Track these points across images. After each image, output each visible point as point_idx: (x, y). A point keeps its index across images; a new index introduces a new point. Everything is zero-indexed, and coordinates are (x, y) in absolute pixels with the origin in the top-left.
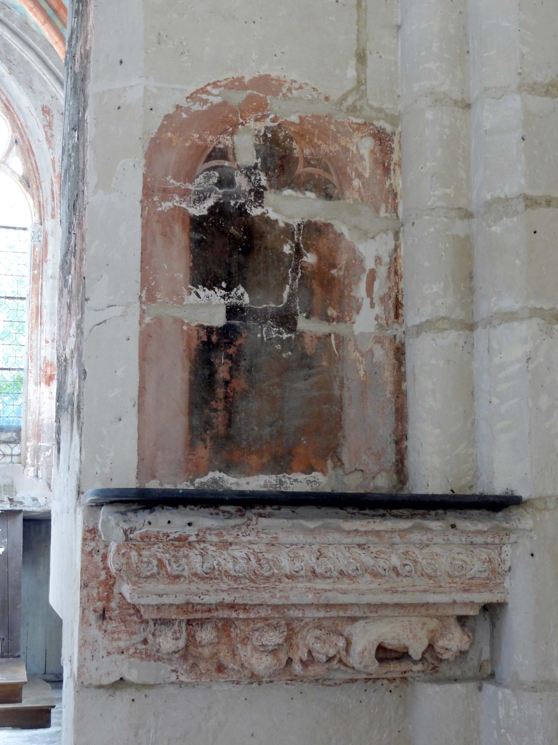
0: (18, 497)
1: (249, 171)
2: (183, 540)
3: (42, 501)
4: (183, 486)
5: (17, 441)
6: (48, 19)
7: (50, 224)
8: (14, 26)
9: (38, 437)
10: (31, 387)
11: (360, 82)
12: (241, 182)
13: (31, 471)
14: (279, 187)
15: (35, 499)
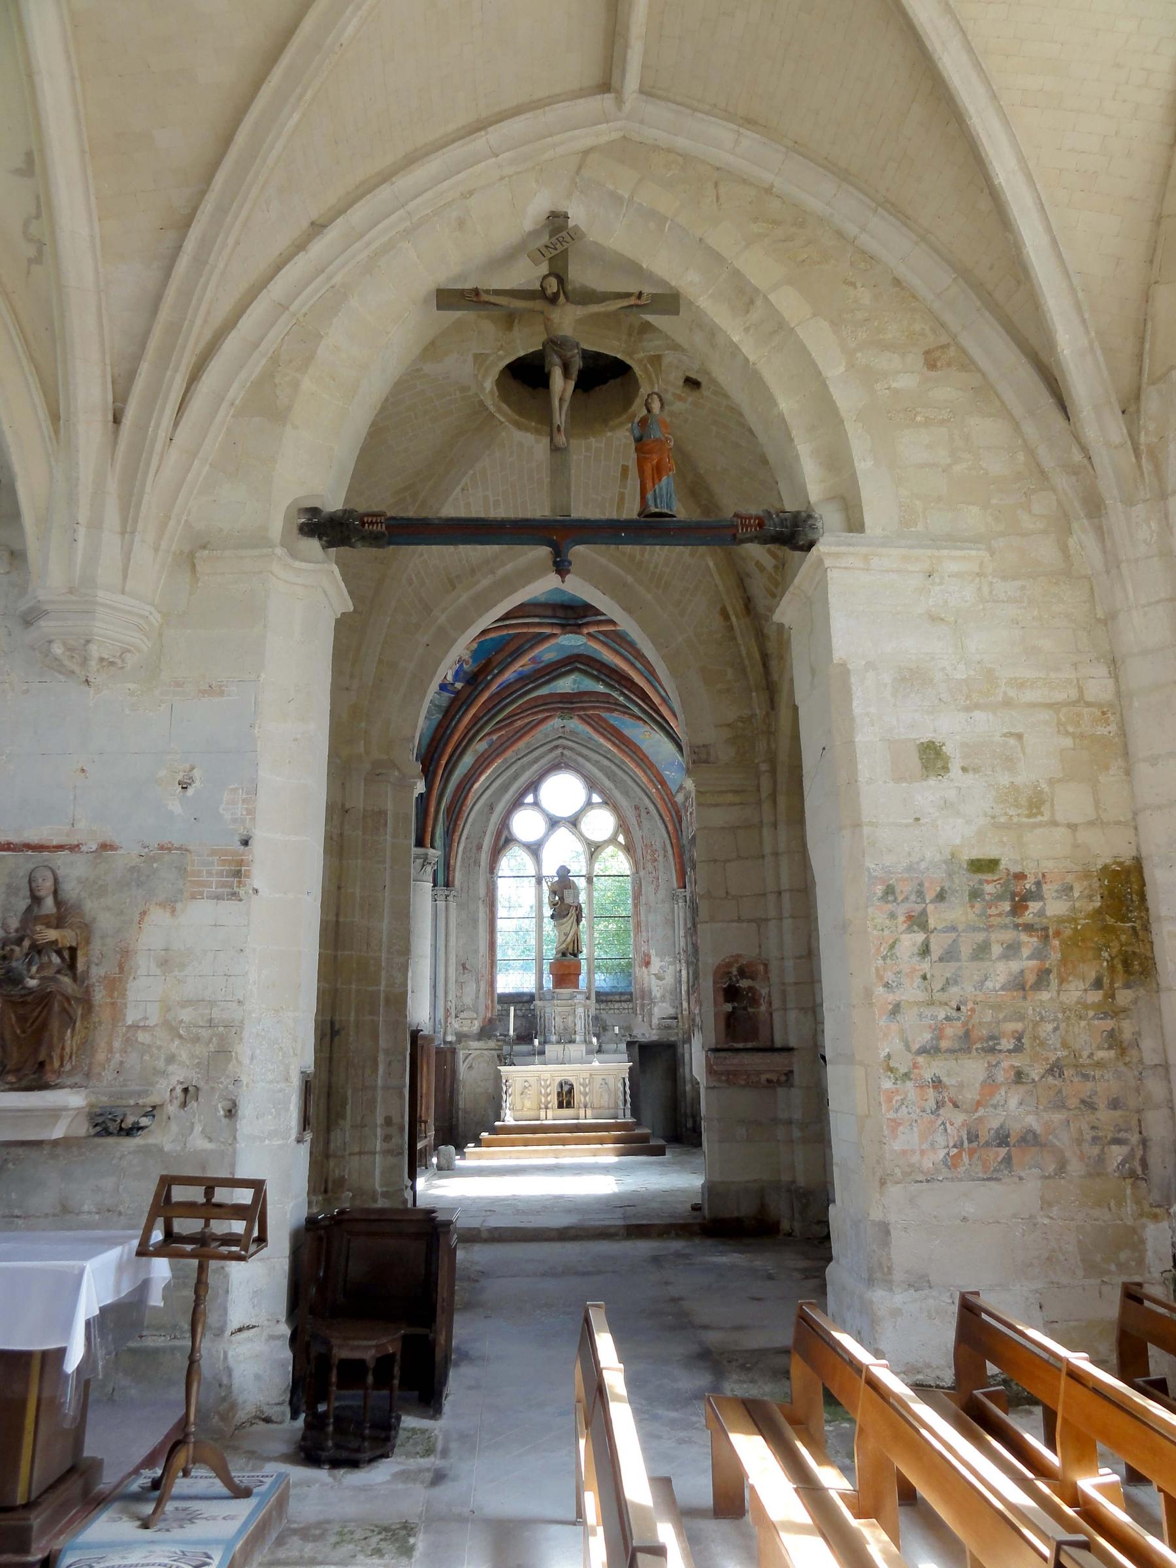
0: (634, 1033)
1: (736, 976)
2: (725, 1058)
3: (647, 1035)
4: (726, 1046)
5: (630, 1001)
6: (638, 765)
7: (642, 873)
8: (617, 762)
9: (643, 998)
10: (637, 969)
11: (760, 954)
12: (734, 979)
13: (640, 1019)
14: (742, 978)
15: (643, 1034)
